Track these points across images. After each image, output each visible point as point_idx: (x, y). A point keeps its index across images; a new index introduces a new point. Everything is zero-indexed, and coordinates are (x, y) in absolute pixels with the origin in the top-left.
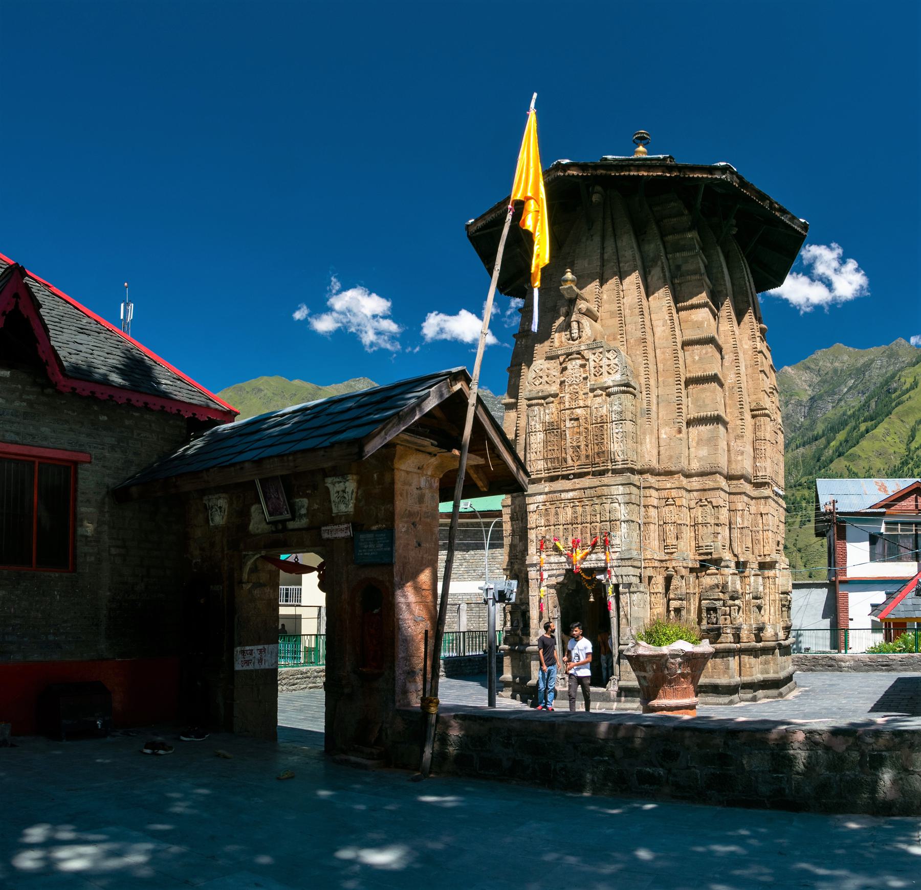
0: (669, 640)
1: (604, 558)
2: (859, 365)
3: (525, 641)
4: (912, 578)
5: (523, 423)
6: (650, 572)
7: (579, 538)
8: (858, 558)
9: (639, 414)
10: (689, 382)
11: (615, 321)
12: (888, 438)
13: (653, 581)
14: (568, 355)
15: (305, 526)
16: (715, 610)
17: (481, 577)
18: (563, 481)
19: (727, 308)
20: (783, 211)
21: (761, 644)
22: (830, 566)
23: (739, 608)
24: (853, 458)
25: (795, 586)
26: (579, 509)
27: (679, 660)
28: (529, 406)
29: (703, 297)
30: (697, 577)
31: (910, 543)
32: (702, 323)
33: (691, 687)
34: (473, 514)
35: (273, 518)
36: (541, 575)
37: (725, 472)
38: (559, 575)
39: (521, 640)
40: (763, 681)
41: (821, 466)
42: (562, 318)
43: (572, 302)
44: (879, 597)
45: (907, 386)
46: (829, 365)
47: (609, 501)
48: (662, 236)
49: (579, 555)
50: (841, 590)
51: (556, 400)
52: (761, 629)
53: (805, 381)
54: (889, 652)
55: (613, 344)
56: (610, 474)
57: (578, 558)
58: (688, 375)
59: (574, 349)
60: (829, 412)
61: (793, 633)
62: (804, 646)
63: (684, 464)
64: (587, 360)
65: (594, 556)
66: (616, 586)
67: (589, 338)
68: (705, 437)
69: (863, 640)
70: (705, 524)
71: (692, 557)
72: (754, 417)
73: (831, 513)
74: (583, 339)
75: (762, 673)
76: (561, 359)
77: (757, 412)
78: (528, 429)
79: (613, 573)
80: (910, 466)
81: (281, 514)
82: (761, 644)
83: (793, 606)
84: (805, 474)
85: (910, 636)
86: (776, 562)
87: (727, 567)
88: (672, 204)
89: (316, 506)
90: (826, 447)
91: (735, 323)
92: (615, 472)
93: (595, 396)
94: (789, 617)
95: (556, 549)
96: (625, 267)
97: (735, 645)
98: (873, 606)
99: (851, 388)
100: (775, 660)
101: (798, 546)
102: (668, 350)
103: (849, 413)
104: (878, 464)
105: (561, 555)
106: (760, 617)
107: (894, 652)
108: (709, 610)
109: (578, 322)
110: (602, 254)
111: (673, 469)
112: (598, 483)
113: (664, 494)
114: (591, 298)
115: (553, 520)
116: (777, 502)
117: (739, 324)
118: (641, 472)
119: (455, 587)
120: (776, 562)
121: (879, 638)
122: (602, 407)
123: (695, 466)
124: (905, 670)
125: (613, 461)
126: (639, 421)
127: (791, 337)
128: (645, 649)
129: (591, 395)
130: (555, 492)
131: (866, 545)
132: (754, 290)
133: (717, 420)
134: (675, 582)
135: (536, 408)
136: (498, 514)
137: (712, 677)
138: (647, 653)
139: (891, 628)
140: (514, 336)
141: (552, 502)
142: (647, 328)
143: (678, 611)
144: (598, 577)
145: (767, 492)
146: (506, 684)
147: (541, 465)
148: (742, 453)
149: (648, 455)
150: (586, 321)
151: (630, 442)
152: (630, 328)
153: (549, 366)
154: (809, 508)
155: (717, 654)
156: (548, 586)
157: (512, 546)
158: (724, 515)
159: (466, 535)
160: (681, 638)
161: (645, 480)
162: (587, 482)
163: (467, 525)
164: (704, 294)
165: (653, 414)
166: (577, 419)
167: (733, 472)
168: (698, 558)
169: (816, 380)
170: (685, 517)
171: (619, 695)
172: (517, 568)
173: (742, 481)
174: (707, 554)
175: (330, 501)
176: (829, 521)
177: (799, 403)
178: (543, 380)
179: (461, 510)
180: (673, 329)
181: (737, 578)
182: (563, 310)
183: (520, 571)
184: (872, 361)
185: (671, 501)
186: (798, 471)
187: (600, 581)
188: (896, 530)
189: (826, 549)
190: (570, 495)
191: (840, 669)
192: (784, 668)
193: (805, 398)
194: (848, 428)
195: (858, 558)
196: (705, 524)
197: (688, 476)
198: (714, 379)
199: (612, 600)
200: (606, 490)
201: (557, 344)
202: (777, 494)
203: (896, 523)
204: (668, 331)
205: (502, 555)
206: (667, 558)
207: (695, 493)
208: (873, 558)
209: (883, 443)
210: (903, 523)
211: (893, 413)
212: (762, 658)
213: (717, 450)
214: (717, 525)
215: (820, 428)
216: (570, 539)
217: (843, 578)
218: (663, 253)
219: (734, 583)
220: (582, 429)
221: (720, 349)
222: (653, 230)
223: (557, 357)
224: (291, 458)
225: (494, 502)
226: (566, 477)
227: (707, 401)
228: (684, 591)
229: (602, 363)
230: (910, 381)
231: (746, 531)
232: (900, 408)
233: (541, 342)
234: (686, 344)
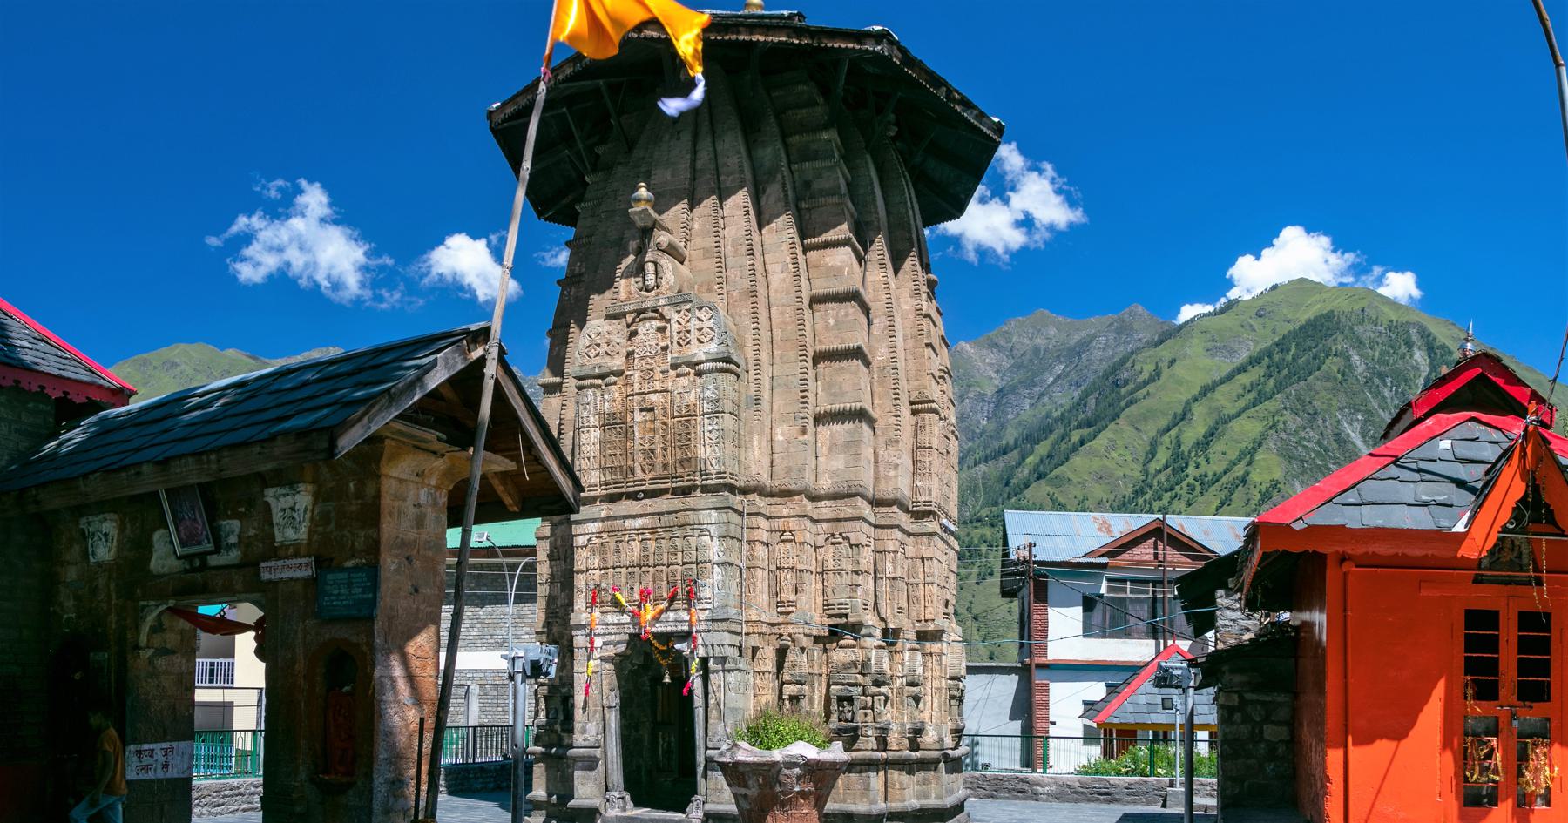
0: (784, 741)
2: (1072, 343)
3: (566, 742)
4: (1147, 665)
5: (570, 413)
6: (754, 641)
7: (651, 587)
8: (1065, 631)
9: (743, 405)
10: (819, 358)
11: (711, 264)
12: (1114, 454)
13: (759, 655)
14: (640, 312)
15: (236, 562)
16: (850, 700)
17: (501, 645)
18: (629, 502)
19: (879, 249)
20: (967, 104)
21: (918, 754)
22: (1022, 637)
23: (887, 698)
24: (1060, 482)
25: (971, 670)
26: (652, 545)
27: (797, 771)
28: (580, 388)
29: (843, 231)
30: (825, 650)
31: (1144, 611)
32: (841, 269)
33: (815, 812)
34: (491, 551)
35: (186, 551)
36: (592, 642)
37: (870, 493)
38: (619, 643)
39: (560, 739)
40: (920, 810)
41: (1011, 492)
42: (632, 257)
43: (647, 232)
44: (1096, 690)
45: (1145, 375)
46: (1027, 341)
47: (697, 533)
48: (784, 136)
49: (649, 612)
50: (1038, 678)
51: (621, 381)
52: (918, 731)
53: (991, 365)
54: (1109, 774)
55: (707, 298)
56: (698, 493)
57: (649, 617)
58: (818, 348)
59: (649, 304)
60: (1025, 411)
61: (966, 741)
62: (982, 760)
63: (808, 480)
64: (668, 321)
65: (671, 615)
66: (704, 661)
67: (671, 288)
68: (841, 440)
69: (1069, 755)
70: (839, 572)
71: (817, 619)
72: (914, 412)
73: (1026, 562)
74: (662, 289)
75: (918, 798)
76: (629, 318)
77: (920, 406)
78: (579, 422)
79: (700, 641)
80: (1147, 497)
81: (199, 543)
82: (918, 754)
83: (966, 699)
84: (987, 504)
85: (1143, 751)
86: (943, 631)
87: (870, 636)
88: (801, 87)
89: (252, 532)
90: (1019, 465)
91: (891, 271)
92: (706, 489)
93: (678, 376)
94: (960, 714)
95: (616, 603)
96: (727, 181)
97: (878, 755)
98: (1086, 703)
99: (1059, 377)
100: (938, 779)
101: (975, 611)
102: (788, 309)
103: (1055, 415)
104: (1098, 491)
105: (623, 612)
106: (916, 713)
107: (1118, 774)
108: (841, 700)
109: (656, 264)
110: (693, 161)
111: (793, 487)
112: (681, 506)
113: (779, 524)
114: (676, 227)
115: (611, 560)
116: (946, 542)
117: (896, 274)
118: (744, 491)
119: (464, 660)
120: (943, 631)
121: (1095, 751)
122: (689, 391)
123: (825, 484)
124: (1134, 802)
125: (704, 473)
126: (743, 415)
127: (973, 295)
128: (747, 753)
129: (672, 373)
130: (615, 518)
131: (1077, 612)
132: (919, 222)
133: (860, 415)
134: (792, 657)
135: (590, 392)
136: (531, 551)
137: (844, 801)
138: (750, 759)
139: (1115, 738)
140: (559, 282)
141: (611, 533)
142: (758, 274)
143: (795, 699)
144: (677, 646)
145: (931, 526)
146: (537, 805)
148: (896, 467)
149: (755, 465)
150: (667, 263)
151: (729, 444)
152: (733, 274)
154: (992, 554)
155: (851, 766)
156: (602, 659)
157: (551, 599)
158: (867, 558)
159: (483, 581)
160: (801, 739)
161: (750, 503)
162: (663, 503)
163: (481, 567)
164: (845, 226)
165: (765, 406)
166: (651, 410)
167: (881, 495)
168: (827, 621)
169: (1007, 363)
170: (809, 560)
172: (558, 630)
173: (895, 508)
174: (840, 616)
175: (271, 524)
176: (1022, 573)
177: (981, 398)
178: (601, 350)
179: (473, 544)
180: (797, 277)
181: (885, 653)
182: (633, 245)
183: (562, 636)
184: (1093, 338)
185: (788, 536)
186: (977, 500)
187: (680, 652)
188: (1123, 590)
189: (1016, 617)
190: (639, 522)
191: (1035, 797)
192: (951, 792)
193: (990, 391)
194: (1053, 437)
195: (1065, 631)
196: (839, 572)
197: (814, 498)
198: (857, 353)
199: (697, 685)
201: (623, 295)
202: (946, 530)
203: (1124, 581)
204: (790, 280)
205: (536, 613)
206: (780, 620)
207: (825, 525)
208: (1088, 631)
209: (1106, 462)
210: (1133, 581)
211: (1122, 416)
212: (920, 775)
213: (858, 460)
214: (856, 573)
215: (1011, 436)
216: (637, 588)
217: (1042, 660)
218: (784, 162)
219: (879, 660)
220: (658, 424)
221: (866, 310)
222: (771, 126)
223: (624, 315)
224: (213, 457)
225: (525, 531)
226: (632, 496)
227: (846, 388)
228: (805, 670)
230: (1149, 368)
231: (899, 583)
232: (1133, 408)
233: (601, 291)
234: (816, 300)
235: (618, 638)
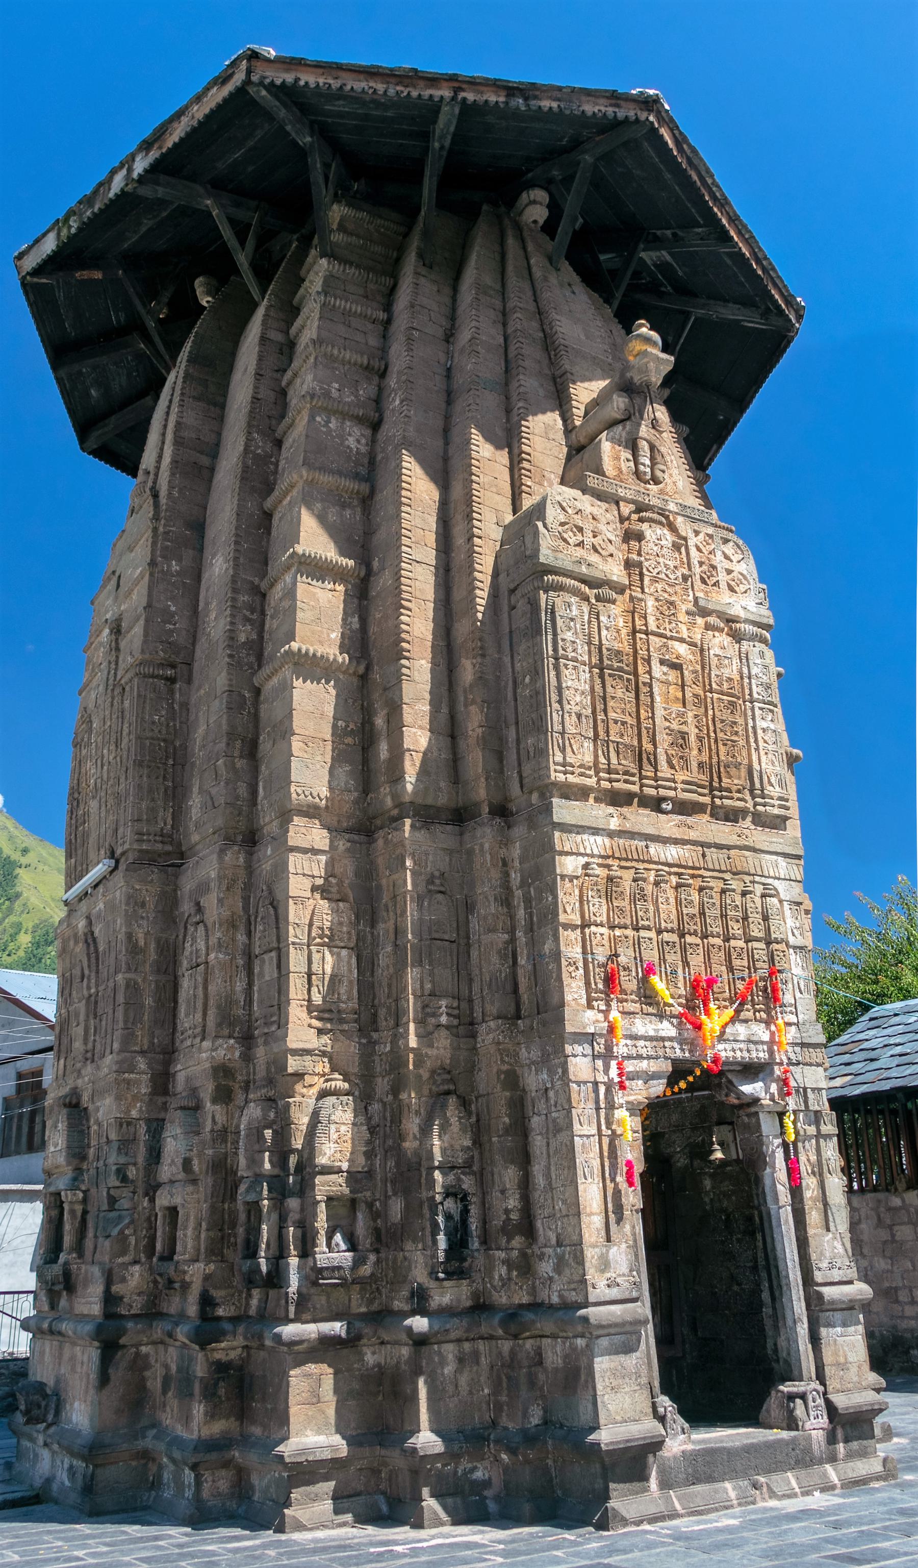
1: (766, 1037)
38: (655, 1076)
49: (714, 1020)
65: (741, 1030)
95: (648, 996)
105: (661, 1016)
130: (632, 835)
153: (595, 511)
171: (831, 1439)
190: (672, 853)
200: (750, 861)
226: (655, 805)
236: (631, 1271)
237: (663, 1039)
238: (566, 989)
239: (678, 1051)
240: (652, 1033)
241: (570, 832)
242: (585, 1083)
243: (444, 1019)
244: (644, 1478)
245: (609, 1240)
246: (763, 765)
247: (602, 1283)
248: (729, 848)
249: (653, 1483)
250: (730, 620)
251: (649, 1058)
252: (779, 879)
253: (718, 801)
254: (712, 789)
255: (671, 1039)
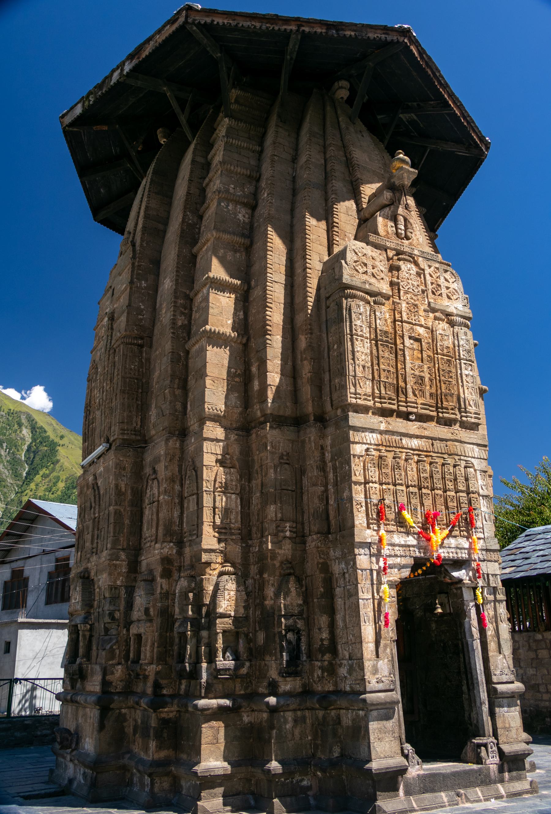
1: (467, 545)
49: (438, 535)
65: (452, 542)
95: (401, 522)
105: (408, 533)
130: (393, 433)
147: (367, 387)
153: (374, 254)
171: (501, 770)
190: (415, 443)
226: (406, 416)
229: (442, 281)
235: (403, 561)
236: (390, 674)
237: (409, 546)
238: (355, 518)
239: (417, 552)
240: (403, 543)
241: (359, 431)
242: (366, 570)
243: (288, 534)
244: (397, 790)
245: (377, 656)
246: (466, 395)
247: (374, 681)
248: (447, 440)
249: (401, 792)
250: (448, 315)
251: (401, 556)
252: (474, 458)
253: (441, 415)
254: (437, 408)
255: (413, 546)
